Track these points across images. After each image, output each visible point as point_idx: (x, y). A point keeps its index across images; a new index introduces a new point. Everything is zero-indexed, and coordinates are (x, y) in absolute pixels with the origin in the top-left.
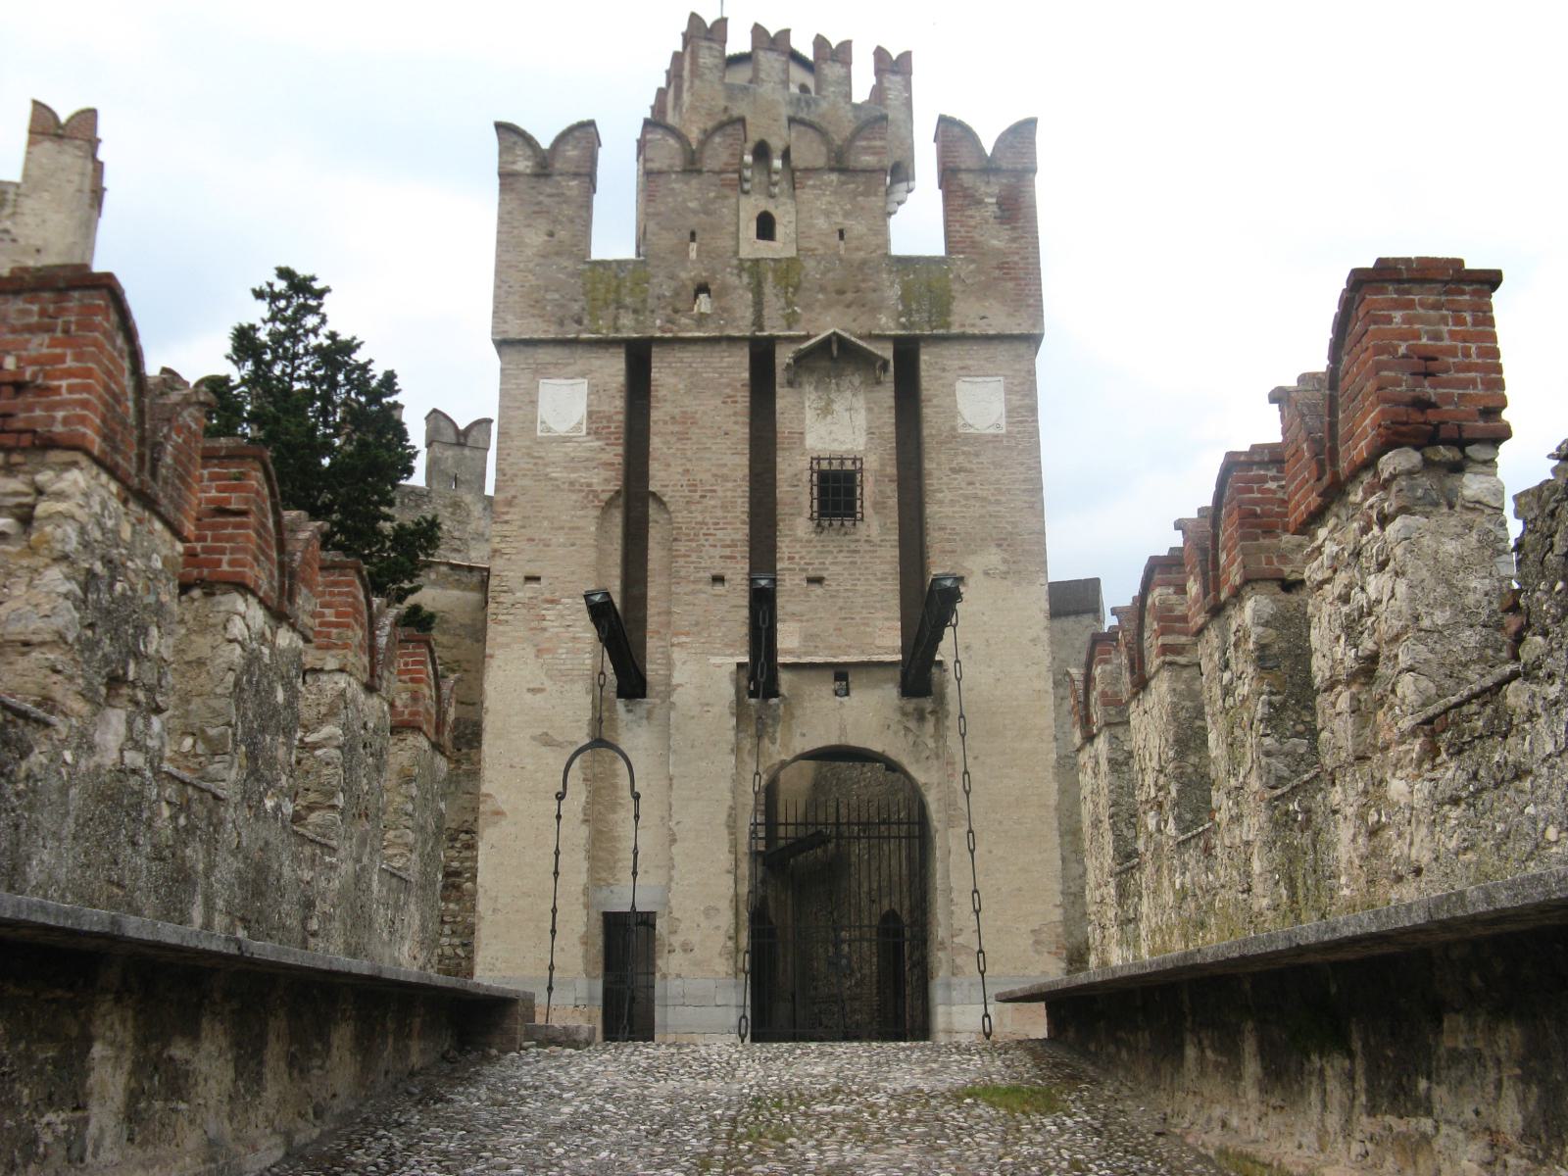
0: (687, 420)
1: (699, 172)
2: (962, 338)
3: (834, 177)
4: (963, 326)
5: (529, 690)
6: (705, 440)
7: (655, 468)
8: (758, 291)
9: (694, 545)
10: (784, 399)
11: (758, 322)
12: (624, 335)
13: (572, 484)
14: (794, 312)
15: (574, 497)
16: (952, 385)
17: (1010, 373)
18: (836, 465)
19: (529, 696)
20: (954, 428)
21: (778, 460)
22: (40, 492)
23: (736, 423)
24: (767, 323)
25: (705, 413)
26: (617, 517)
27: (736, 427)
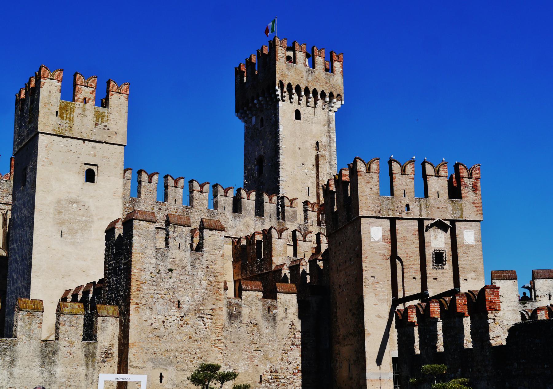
0: (405, 238)
1: (405, 174)
2: (465, 221)
3: (436, 178)
4: (465, 218)
5: (374, 304)
6: (409, 244)
7: (398, 250)
8: (420, 206)
9: (408, 270)
10: (426, 234)
11: (421, 215)
12: (390, 216)
13: (380, 254)
14: (428, 212)
15: (381, 257)
16: (463, 232)
17: (475, 229)
18: (438, 252)
19: (374, 306)
20: (463, 243)
21: (426, 249)
22: (495, 316)
23: (416, 240)
24: (422, 215)
25: (409, 237)
26: (389, 261)
27: (416, 241)
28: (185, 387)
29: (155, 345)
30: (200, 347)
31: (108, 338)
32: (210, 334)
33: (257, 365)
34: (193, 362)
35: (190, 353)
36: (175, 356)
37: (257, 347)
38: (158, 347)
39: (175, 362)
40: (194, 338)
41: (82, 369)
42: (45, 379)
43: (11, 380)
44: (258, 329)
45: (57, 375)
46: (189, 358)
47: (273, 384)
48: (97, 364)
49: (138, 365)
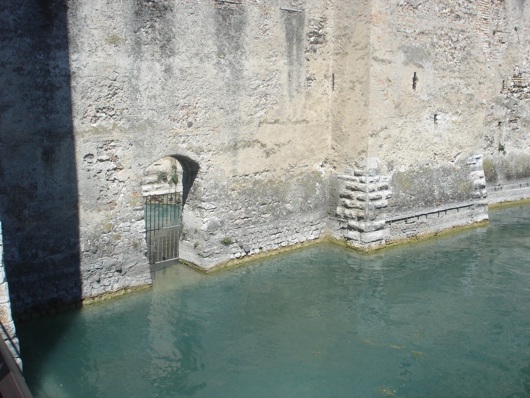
28: (444, 98)
29: (408, 20)
30: (463, 29)
31: (319, 7)
32: (475, 7)
33: (500, 65)
34: (455, 56)
35: (452, 39)
36: (433, 45)
37: (501, 36)
38: (411, 24)
39: (433, 54)
40: (457, 13)
41: (282, 62)
42: (226, 80)
43: (169, 83)
44: (504, 8)
45: (245, 73)
46: (449, 47)
47: (515, 95)
48: (304, 55)
49: (384, 58)
